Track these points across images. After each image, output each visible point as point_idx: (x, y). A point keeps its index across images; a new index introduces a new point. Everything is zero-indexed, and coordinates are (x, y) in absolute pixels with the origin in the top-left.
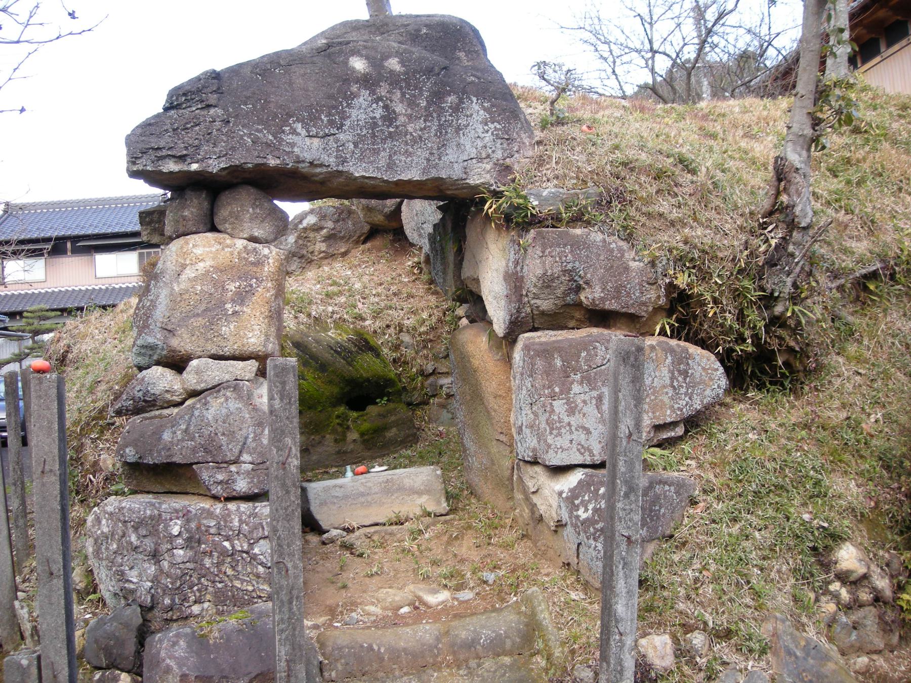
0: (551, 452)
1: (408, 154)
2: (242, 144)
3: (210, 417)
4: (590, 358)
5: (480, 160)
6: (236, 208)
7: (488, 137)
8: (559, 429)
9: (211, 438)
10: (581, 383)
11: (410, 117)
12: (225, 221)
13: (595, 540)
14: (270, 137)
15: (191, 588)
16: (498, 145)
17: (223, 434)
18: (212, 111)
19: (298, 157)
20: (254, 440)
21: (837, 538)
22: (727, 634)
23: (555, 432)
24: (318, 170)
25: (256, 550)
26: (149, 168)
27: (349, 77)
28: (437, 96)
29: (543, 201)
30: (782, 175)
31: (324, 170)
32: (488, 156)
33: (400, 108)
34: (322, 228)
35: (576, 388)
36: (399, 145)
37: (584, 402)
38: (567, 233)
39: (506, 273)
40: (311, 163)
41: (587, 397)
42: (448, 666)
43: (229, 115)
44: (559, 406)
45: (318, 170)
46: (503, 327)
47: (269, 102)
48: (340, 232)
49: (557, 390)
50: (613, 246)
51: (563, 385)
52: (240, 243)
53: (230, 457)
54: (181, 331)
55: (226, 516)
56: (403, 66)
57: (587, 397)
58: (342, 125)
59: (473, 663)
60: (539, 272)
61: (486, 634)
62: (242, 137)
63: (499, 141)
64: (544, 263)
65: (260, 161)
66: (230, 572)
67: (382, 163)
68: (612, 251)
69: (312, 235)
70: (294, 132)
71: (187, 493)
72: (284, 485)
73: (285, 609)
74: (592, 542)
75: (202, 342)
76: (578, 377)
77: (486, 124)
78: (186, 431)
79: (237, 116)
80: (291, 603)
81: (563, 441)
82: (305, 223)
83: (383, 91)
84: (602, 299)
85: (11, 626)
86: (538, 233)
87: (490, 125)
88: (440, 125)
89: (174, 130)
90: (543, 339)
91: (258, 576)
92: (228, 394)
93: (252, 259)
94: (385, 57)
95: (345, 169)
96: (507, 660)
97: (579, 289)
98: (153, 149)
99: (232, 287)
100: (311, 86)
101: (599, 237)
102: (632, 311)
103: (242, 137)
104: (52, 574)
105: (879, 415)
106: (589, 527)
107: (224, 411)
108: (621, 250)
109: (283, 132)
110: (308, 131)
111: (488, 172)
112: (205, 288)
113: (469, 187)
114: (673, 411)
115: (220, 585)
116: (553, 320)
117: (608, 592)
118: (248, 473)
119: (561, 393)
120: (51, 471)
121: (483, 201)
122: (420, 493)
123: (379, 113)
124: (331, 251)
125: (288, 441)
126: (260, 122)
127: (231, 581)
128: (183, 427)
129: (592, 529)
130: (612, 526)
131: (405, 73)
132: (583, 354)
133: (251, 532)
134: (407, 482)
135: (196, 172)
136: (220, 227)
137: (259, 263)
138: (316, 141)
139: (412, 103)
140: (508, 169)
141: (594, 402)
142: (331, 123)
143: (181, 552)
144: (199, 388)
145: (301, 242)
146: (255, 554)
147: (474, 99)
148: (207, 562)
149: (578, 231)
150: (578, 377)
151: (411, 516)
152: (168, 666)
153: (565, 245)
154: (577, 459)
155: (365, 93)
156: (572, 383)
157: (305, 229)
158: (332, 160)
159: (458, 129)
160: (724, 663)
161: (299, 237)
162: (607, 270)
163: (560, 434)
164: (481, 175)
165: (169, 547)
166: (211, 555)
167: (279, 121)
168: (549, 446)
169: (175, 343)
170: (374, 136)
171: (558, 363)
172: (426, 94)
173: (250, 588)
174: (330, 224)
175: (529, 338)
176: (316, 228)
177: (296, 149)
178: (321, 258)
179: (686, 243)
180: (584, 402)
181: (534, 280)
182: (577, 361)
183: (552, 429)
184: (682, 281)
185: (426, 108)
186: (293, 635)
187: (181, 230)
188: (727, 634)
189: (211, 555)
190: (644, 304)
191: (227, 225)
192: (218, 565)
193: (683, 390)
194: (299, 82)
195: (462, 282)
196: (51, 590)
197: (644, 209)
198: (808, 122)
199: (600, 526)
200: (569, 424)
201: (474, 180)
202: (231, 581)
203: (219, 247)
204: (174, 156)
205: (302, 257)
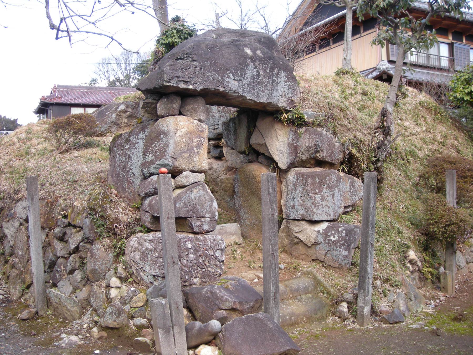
0: (315, 215)
1: (263, 91)
2: (209, 79)
3: (193, 197)
4: (330, 179)
5: (282, 96)
6: (195, 106)
7: (286, 88)
8: (318, 206)
9: (194, 206)
10: (327, 188)
11: (264, 76)
12: (188, 111)
13: (340, 248)
14: (220, 78)
15: (194, 271)
16: (290, 91)
17: (199, 205)
18: (195, 63)
19: (230, 88)
20: (210, 208)
21: (408, 247)
22: (387, 280)
23: (317, 207)
24: (235, 94)
25: (217, 255)
26: (174, 85)
27: (245, 57)
28: (272, 69)
29: (309, 116)
30: (384, 114)
31: (237, 94)
32: (285, 95)
33: (261, 72)
34: (127, 112)
35: (324, 191)
36: (260, 87)
37: (327, 196)
38: (316, 130)
39: (289, 143)
40: (234, 91)
41: (328, 194)
42: (291, 299)
43: (201, 66)
44: (318, 197)
45: (235, 94)
46: (286, 165)
47: (217, 62)
48: (134, 114)
49: (317, 191)
50: (329, 136)
51: (320, 189)
52: (196, 122)
53: (202, 215)
54: (179, 159)
55: (205, 241)
56: (263, 54)
57: (328, 194)
58: (245, 76)
59: (299, 297)
60: (307, 144)
61: (302, 286)
62: (208, 76)
63: (290, 90)
64: (309, 141)
65: (216, 88)
66: (208, 264)
67: (255, 94)
68: (329, 138)
69: (122, 114)
70: (229, 77)
71: (183, 232)
72: (273, 223)
73: (274, 272)
74: (338, 248)
75: (188, 165)
76: (325, 186)
77: (286, 82)
78: (184, 203)
79: (204, 67)
80: (275, 269)
81: (320, 211)
82: (120, 109)
83: (257, 63)
84: (326, 157)
85: (43, 302)
86: (308, 129)
87: (287, 83)
88: (273, 81)
89: (182, 69)
90: (302, 171)
91: (217, 266)
92: (200, 187)
93: (200, 129)
94: (256, 50)
95: (245, 95)
96: (310, 295)
97: (318, 151)
98: (177, 77)
99: (195, 140)
100: (232, 58)
101: (324, 132)
102: (333, 162)
103: (208, 76)
104: (174, 263)
105: (403, 206)
106: (337, 243)
107: (198, 195)
108: (331, 138)
109: (225, 76)
110: (234, 78)
111: (284, 102)
112: (187, 140)
113: (278, 107)
114: (351, 201)
115: (204, 270)
116: (303, 164)
117: (364, 264)
118: (208, 222)
119: (319, 192)
120: (171, 217)
121: (282, 113)
122: (233, 234)
123: (255, 73)
124: (129, 123)
125: (274, 205)
126: (214, 70)
127: (207, 268)
128: (183, 201)
129: (338, 244)
130: (366, 240)
131: (264, 58)
132: (327, 178)
133: (214, 247)
134: (228, 230)
135: (191, 89)
136: (185, 114)
137: (202, 131)
138: (236, 82)
139: (265, 71)
140: (292, 102)
141: (331, 196)
142: (241, 75)
143: (192, 256)
144: (186, 184)
145: (118, 117)
146: (217, 256)
147: (283, 71)
148: (201, 260)
149: (319, 129)
150: (325, 186)
151: (230, 244)
152: (226, 298)
153: (317, 135)
154: (326, 218)
155: (252, 64)
156: (323, 189)
157: (120, 111)
158: (240, 91)
159: (278, 83)
160: (389, 291)
161: (117, 115)
162: (328, 146)
163: (318, 208)
164: (282, 103)
165: (187, 253)
166: (202, 257)
167: (223, 71)
168: (314, 213)
169: (177, 164)
170: (254, 83)
171: (317, 180)
172: (269, 67)
173: (213, 271)
174: (130, 110)
175: (297, 170)
176: (124, 111)
177: (229, 85)
178: (125, 126)
179: (355, 137)
180: (327, 196)
181: (305, 147)
182: (325, 180)
183: (315, 206)
184: (354, 151)
185: (269, 73)
186: (276, 282)
187: (171, 113)
188: (387, 280)
189: (202, 257)
190: (338, 159)
191: (188, 113)
192: (204, 261)
193: (354, 193)
194: (226, 55)
195: (251, 146)
196: (174, 270)
197: (340, 123)
198: (395, 96)
199: (342, 242)
200: (322, 204)
201: (280, 105)
202: (207, 268)
203: (188, 122)
204: (184, 81)
205: (118, 125)
